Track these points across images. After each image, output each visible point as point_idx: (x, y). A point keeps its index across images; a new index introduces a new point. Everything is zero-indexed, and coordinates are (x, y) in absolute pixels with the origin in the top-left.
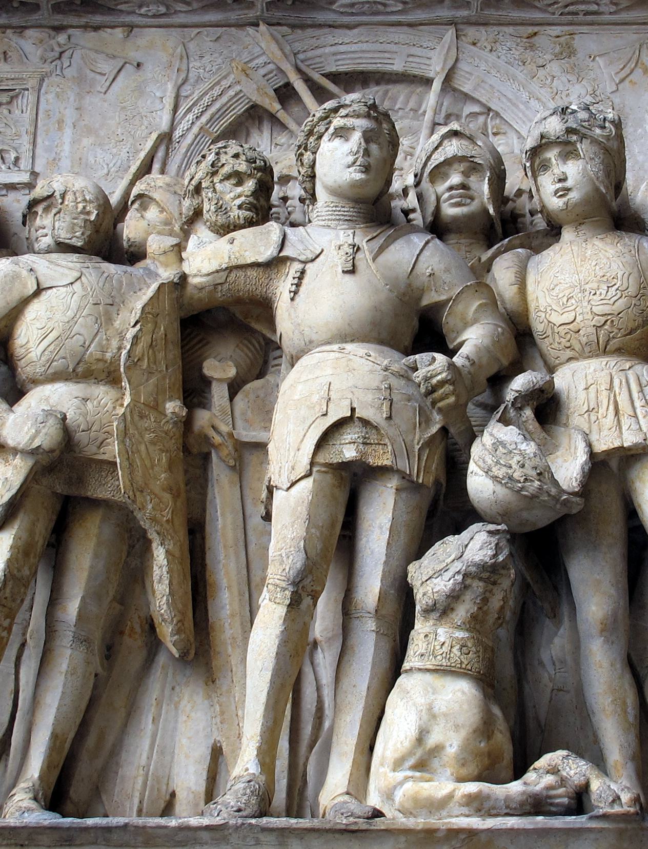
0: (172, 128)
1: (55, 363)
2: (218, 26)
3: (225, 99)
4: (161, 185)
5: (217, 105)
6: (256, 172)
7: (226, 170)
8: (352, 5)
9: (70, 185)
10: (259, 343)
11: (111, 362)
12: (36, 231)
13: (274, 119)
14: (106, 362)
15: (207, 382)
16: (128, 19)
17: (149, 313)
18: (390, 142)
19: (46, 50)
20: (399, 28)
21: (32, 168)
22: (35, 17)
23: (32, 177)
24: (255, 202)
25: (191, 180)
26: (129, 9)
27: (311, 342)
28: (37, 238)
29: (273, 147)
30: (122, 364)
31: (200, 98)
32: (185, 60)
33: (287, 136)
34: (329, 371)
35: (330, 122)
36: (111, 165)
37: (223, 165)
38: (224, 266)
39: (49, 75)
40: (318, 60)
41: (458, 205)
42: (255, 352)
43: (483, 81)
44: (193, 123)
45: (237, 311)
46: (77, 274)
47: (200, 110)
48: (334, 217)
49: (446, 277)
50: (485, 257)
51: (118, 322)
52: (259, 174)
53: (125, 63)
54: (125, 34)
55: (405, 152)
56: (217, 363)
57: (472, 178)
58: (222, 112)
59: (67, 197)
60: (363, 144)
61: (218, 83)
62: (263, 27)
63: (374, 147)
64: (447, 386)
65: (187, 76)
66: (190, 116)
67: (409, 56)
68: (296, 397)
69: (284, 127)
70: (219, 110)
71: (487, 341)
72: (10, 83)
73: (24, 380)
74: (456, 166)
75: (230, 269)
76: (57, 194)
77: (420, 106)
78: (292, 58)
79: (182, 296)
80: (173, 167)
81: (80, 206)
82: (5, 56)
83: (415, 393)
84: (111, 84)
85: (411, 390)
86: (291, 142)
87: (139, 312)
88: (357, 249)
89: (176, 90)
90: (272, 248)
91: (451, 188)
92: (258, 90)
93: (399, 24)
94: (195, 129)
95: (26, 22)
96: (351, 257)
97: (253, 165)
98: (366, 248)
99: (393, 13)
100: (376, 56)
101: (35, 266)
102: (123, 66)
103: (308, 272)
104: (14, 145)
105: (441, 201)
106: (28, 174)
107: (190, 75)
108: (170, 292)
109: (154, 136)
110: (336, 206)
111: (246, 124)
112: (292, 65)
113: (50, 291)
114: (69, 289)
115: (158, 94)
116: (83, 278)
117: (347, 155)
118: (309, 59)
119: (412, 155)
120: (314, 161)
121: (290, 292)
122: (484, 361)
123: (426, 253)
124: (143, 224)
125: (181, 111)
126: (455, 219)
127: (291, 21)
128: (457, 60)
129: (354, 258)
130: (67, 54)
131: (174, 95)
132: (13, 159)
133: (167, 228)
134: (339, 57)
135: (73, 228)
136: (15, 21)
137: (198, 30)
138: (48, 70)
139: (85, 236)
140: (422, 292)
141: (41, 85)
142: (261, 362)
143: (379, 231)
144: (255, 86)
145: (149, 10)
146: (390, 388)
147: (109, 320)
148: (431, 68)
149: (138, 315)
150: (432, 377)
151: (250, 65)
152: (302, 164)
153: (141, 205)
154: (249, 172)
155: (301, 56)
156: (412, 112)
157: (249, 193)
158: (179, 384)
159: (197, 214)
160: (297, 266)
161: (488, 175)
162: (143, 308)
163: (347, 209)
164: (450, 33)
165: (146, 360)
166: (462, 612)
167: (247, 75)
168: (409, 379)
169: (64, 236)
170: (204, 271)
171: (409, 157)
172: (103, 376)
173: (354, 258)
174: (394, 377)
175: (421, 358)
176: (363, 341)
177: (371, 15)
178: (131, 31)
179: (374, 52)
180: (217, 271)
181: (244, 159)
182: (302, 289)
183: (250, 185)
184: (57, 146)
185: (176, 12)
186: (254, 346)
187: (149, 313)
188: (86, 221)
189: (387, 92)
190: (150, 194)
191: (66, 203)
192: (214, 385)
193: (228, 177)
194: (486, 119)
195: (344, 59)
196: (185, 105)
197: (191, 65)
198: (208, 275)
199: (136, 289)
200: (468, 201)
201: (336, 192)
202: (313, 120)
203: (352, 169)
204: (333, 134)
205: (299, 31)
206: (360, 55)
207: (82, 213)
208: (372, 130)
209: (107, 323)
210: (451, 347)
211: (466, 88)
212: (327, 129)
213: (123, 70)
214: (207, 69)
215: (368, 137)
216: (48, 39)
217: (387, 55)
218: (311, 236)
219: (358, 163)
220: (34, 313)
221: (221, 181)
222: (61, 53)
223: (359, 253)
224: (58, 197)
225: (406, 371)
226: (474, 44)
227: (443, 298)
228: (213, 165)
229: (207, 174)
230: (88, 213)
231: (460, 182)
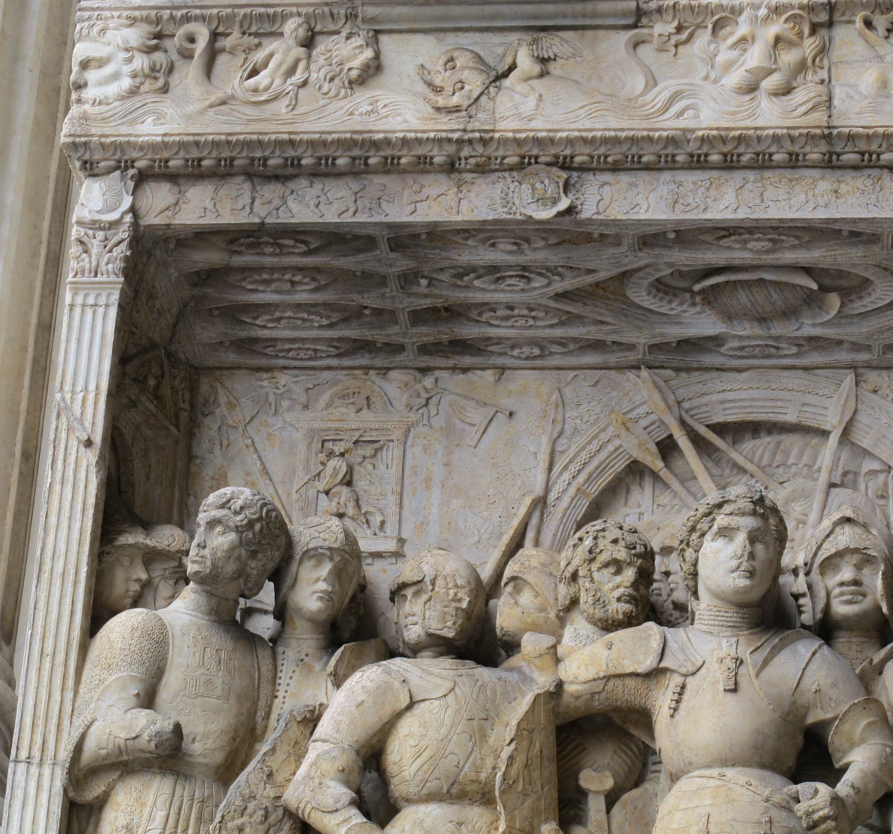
0: (547, 490)
1: (428, 784)
2: (596, 369)
3: (603, 455)
4: (535, 564)
5: (595, 462)
6: (636, 559)
7: (604, 557)
8: (742, 348)
9: (440, 568)
10: (638, 747)
11: (486, 784)
12: (406, 618)
13: (655, 476)
14: (480, 783)
15: (583, 794)
16: (499, 361)
17: (525, 730)
18: (777, 539)
19: (411, 396)
20: (793, 372)
21: (399, 534)
22: (400, 358)
23: (399, 544)
24: (635, 593)
25: (567, 565)
26: (501, 351)
27: (690, 764)
28: (406, 626)
29: (655, 507)
30: (497, 787)
31: (577, 454)
32: (560, 409)
33: (670, 496)
34: (709, 801)
35: (713, 520)
36: (482, 531)
37: (601, 551)
38: (602, 674)
39: (415, 424)
40: (705, 409)
41: (849, 602)
42: (633, 757)
43: (883, 436)
44: (569, 483)
45: (616, 719)
46: (450, 685)
47: (577, 469)
48: (716, 623)
49: (833, 693)
50: (876, 659)
51: (492, 739)
52: (640, 561)
53: (497, 412)
54: (497, 377)
55: (796, 520)
56: (594, 773)
57: (866, 571)
58: (601, 469)
59: (438, 583)
60: (748, 548)
61: (596, 436)
62: (644, 373)
63: (759, 548)
64: (829, 821)
65: (563, 428)
66: (566, 476)
67: (803, 405)
68: (675, 826)
69: (667, 486)
70: (597, 468)
71: (873, 766)
72: (374, 433)
73: (397, 798)
74: (848, 558)
75: (608, 678)
76: (427, 579)
77: (815, 460)
78: (676, 409)
79: (557, 706)
80: (547, 537)
81: (452, 592)
82: (368, 402)
83: (797, 825)
84: (481, 437)
85: (792, 823)
86: (675, 502)
87: (514, 729)
88: (740, 662)
89: (550, 445)
90: (651, 658)
91: (842, 584)
92: (639, 445)
93: (793, 368)
94: (572, 491)
95: (390, 363)
96: (734, 673)
97: (633, 551)
98: (749, 661)
99: (786, 356)
100: (767, 404)
101: (407, 675)
102: (494, 415)
103: (689, 687)
104: (380, 506)
105: (832, 595)
106: (395, 541)
107: (566, 426)
108: (546, 703)
109: (528, 501)
110: (719, 611)
111: (627, 480)
112: (676, 418)
113: (422, 705)
114: (442, 702)
115: (532, 449)
116: (457, 689)
117: (731, 559)
118: (695, 408)
119: (804, 523)
120: (697, 560)
121: (670, 708)
122: (870, 786)
123: (813, 666)
124: (518, 610)
125: (557, 469)
126: (846, 618)
127: (675, 364)
128: (856, 411)
129: (736, 674)
130: (434, 401)
131: (549, 451)
132: (378, 523)
133: (542, 615)
134: (727, 405)
135: (444, 617)
136: (379, 362)
137: (574, 373)
138: (414, 419)
139: (457, 626)
140: (807, 709)
141: (406, 437)
142: (639, 766)
143: (763, 640)
144: (636, 442)
145: (522, 353)
146: (770, 822)
147: (484, 737)
148: (828, 419)
149: (513, 733)
150: (813, 812)
151: (630, 416)
152: (684, 560)
153: (515, 588)
154: (629, 560)
155: (686, 405)
156: (806, 469)
157: (629, 584)
158: (555, 803)
159: (574, 602)
160: (677, 680)
161: (882, 568)
162: (518, 725)
163: (731, 615)
164: (849, 379)
165: (521, 781)
167: (628, 429)
168: (790, 810)
169: (435, 627)
170: (581, 678)
171: (801, 526)
172: (478, 797)
173: (736, 674)
174: (775, 809)
175: (805, 788)
176: (744, 766)
177: (762, 358)
178: (503, 373)
179: (766, 400)
180: (595, 680)
181: (623, 545)
182: (683, 705)
183: (629, 574)
184: (424, 509)
185: (551, 354)
186: (632, 750)
187: (524, 729)
188: (457, 609)
189: (779, 443)
190: (524, 577)
191: (437, 589)
192: (591, 797)
193: (606, 565)
194: (887, 476)
195: (733, 408)
196: (560, 463)
197: (567, 415)
198: (585, 683)
199: (509, 698)
200: (860, 598)
201: (719, 596)
202: (695, 516)
203: (735, 574)
204: (717, 533)
205: (684, 375)
206: (750, 403)
207: (453, 600)
208: (758, 529)
209: (481, 740)
210: (837, 766)
211: (866, 443)
212: (710, 527)
213: (494, 420)
214: (584, 420)
215: (753, 539)
216: (413, 383)
217: (779, 404)
218: (693, 642)
219: (742, 568)
220: (407, 727)
221: (599, 569)
222: (428, 399)
223: (742, 667)
224: (428, 583)
225: (788, 802)
226: (875, 391)
227: (829, 715)
228: (590, 552)
229: (584, 562)
230: (460, 600)
231: (851, 578)
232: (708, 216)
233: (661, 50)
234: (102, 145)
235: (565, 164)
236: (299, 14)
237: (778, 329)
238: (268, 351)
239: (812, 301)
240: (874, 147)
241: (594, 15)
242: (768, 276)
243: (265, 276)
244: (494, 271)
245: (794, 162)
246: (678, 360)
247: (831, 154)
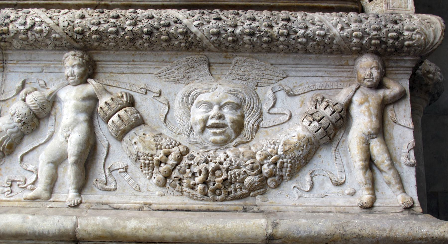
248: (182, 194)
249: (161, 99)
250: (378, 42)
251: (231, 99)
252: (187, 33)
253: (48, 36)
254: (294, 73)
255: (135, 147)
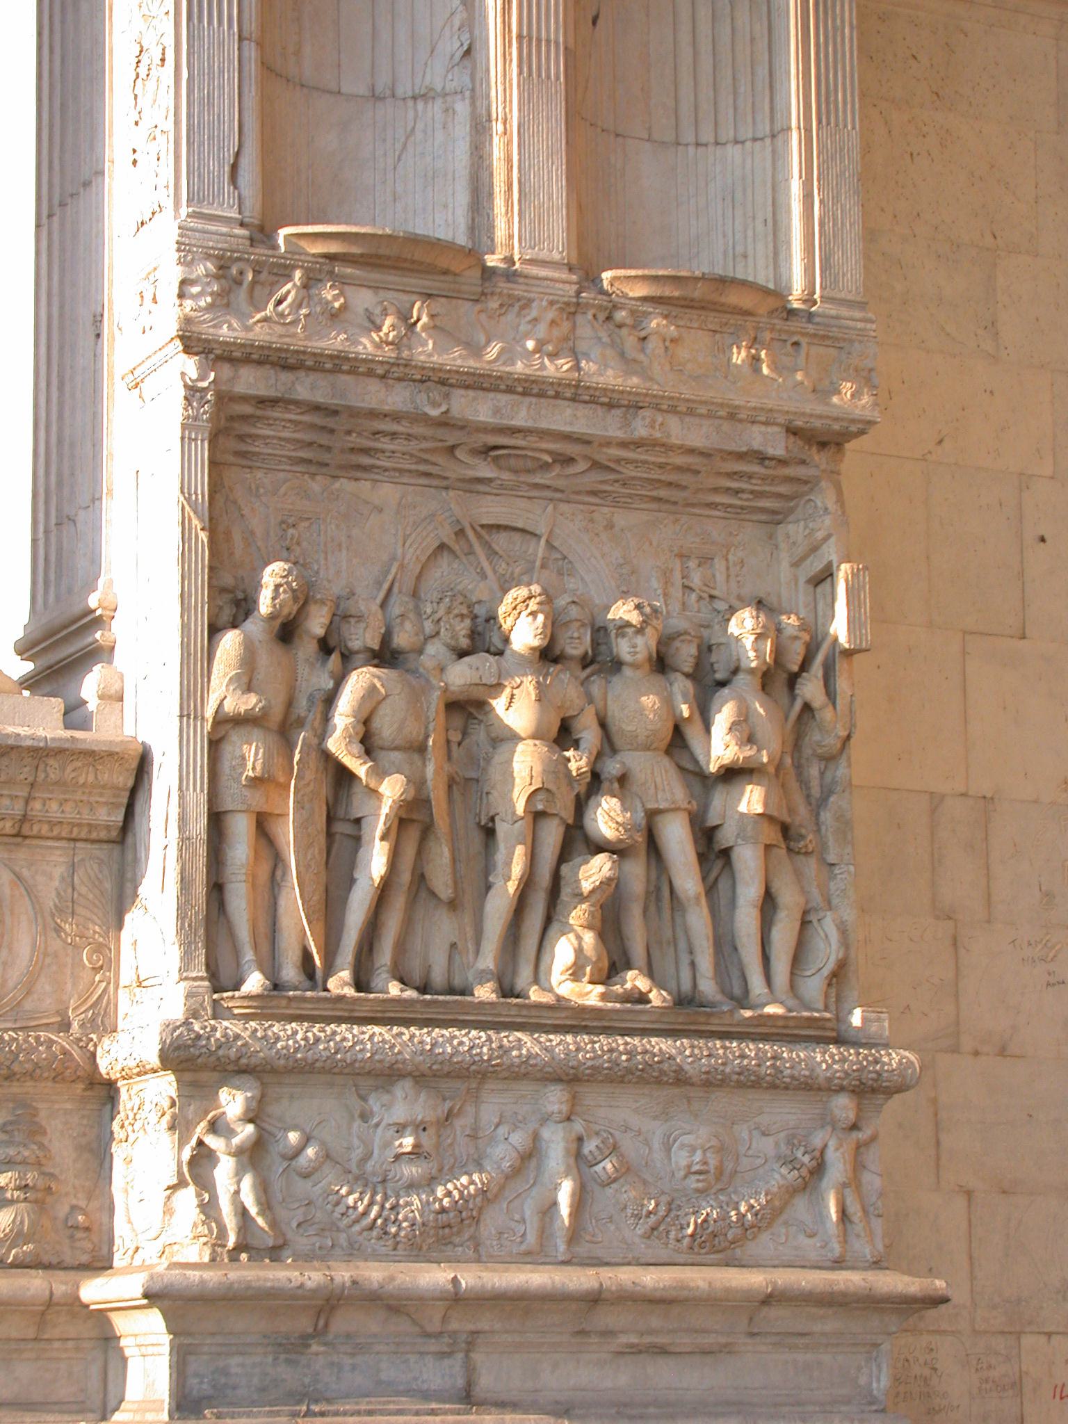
7: (456, 612)
16: (377, 477)
22: (324, 470)
69: (457, 557)
125: (407, 545)
166: (593, 899)
193: (457, 616)
211: (555, 544)
232: (513, 423)
233: (490, 317)
234: (199, 340)
235: (443, 382)
236: (302, 267)
237: (523, 478)
238: (254, 458)
239: (545, 467)
240: (597, 393)
241: (459, 292)
242: (530, 454)
243: (271, 422)
244: (394, 435)
245: (557, 396)
246: (468, 486)
247: (576, 394)
248: (667, 1248)
249: (641, 1138)
250: (857, 1083)
251: (714, 1142)
252: (680, 1070)
253: (541, 1070)
254: (768, 1110)
255: (625, 1196)
